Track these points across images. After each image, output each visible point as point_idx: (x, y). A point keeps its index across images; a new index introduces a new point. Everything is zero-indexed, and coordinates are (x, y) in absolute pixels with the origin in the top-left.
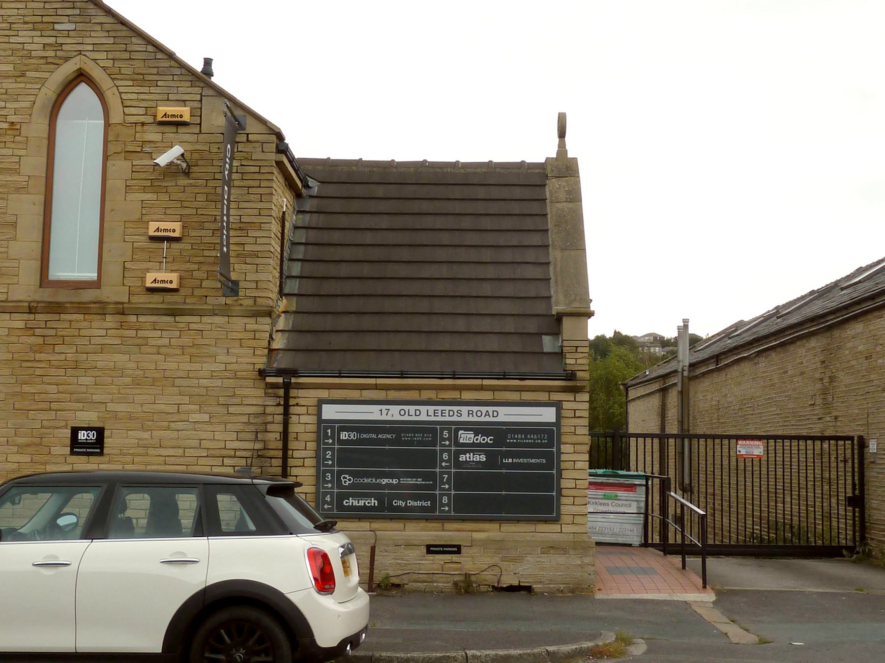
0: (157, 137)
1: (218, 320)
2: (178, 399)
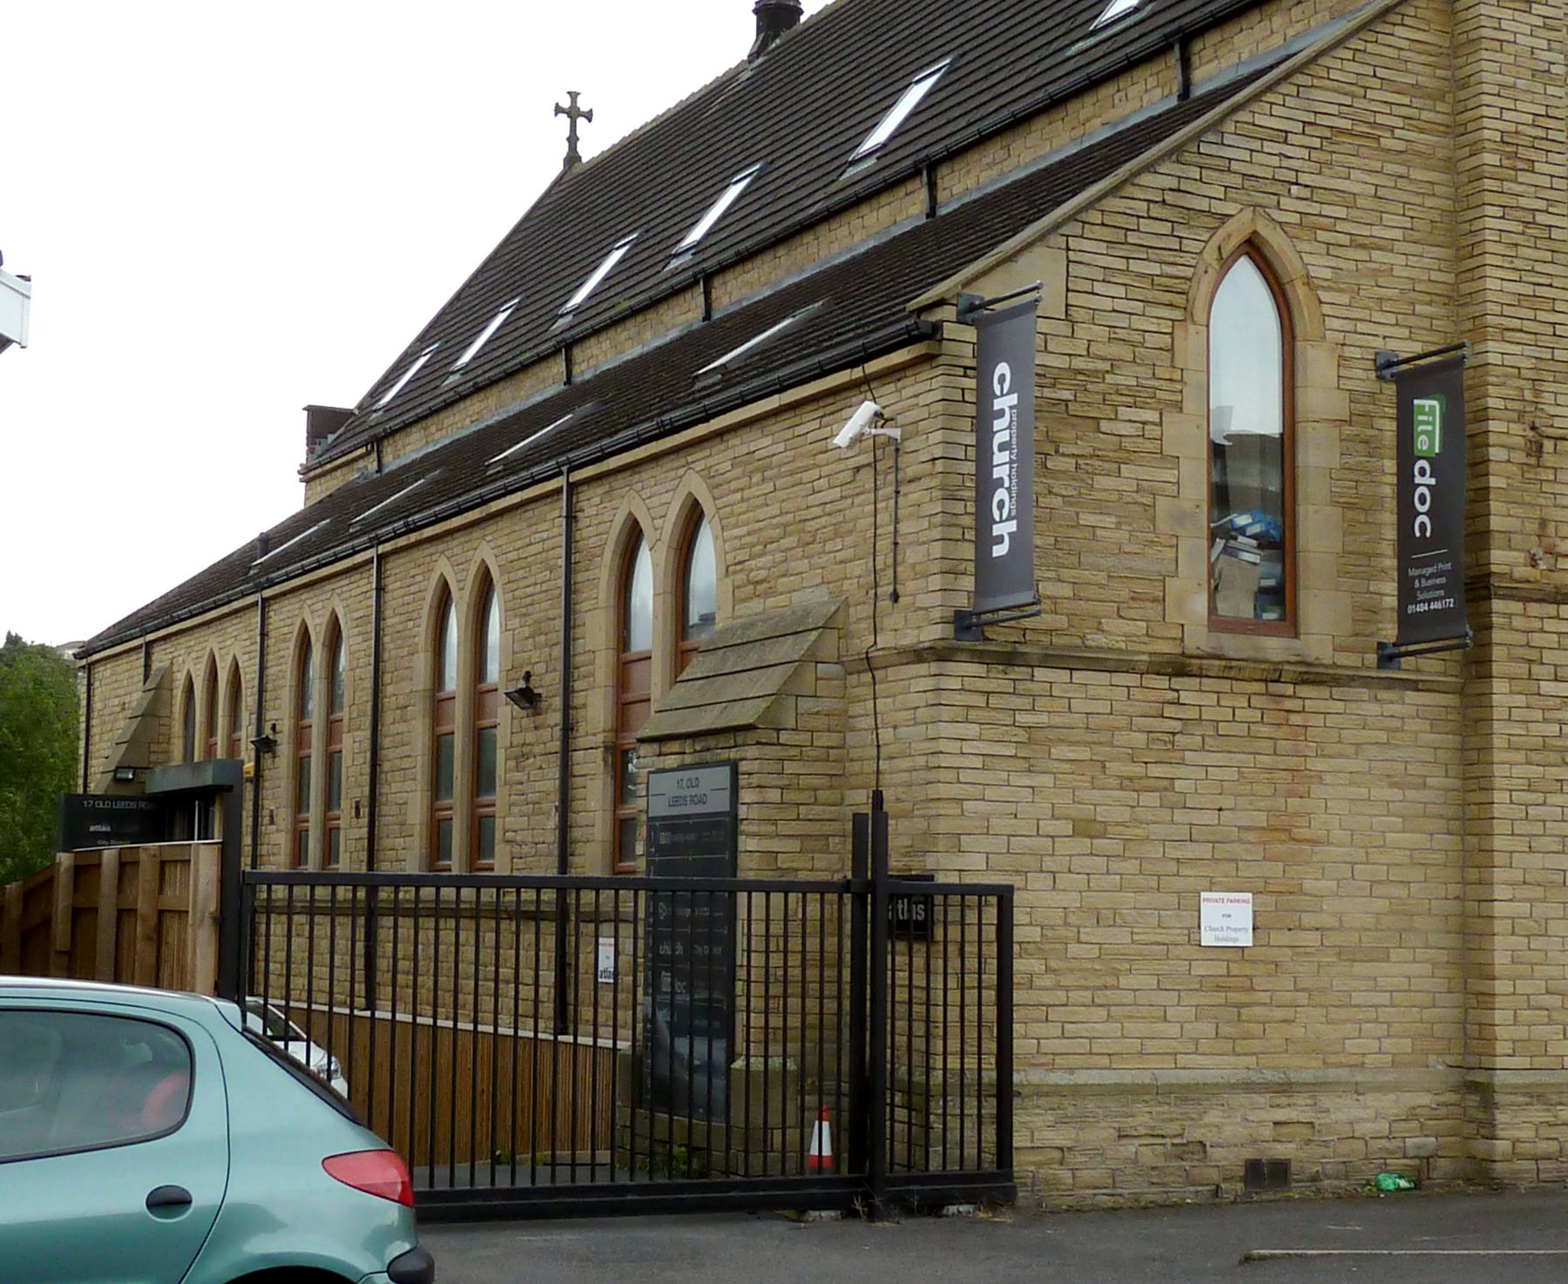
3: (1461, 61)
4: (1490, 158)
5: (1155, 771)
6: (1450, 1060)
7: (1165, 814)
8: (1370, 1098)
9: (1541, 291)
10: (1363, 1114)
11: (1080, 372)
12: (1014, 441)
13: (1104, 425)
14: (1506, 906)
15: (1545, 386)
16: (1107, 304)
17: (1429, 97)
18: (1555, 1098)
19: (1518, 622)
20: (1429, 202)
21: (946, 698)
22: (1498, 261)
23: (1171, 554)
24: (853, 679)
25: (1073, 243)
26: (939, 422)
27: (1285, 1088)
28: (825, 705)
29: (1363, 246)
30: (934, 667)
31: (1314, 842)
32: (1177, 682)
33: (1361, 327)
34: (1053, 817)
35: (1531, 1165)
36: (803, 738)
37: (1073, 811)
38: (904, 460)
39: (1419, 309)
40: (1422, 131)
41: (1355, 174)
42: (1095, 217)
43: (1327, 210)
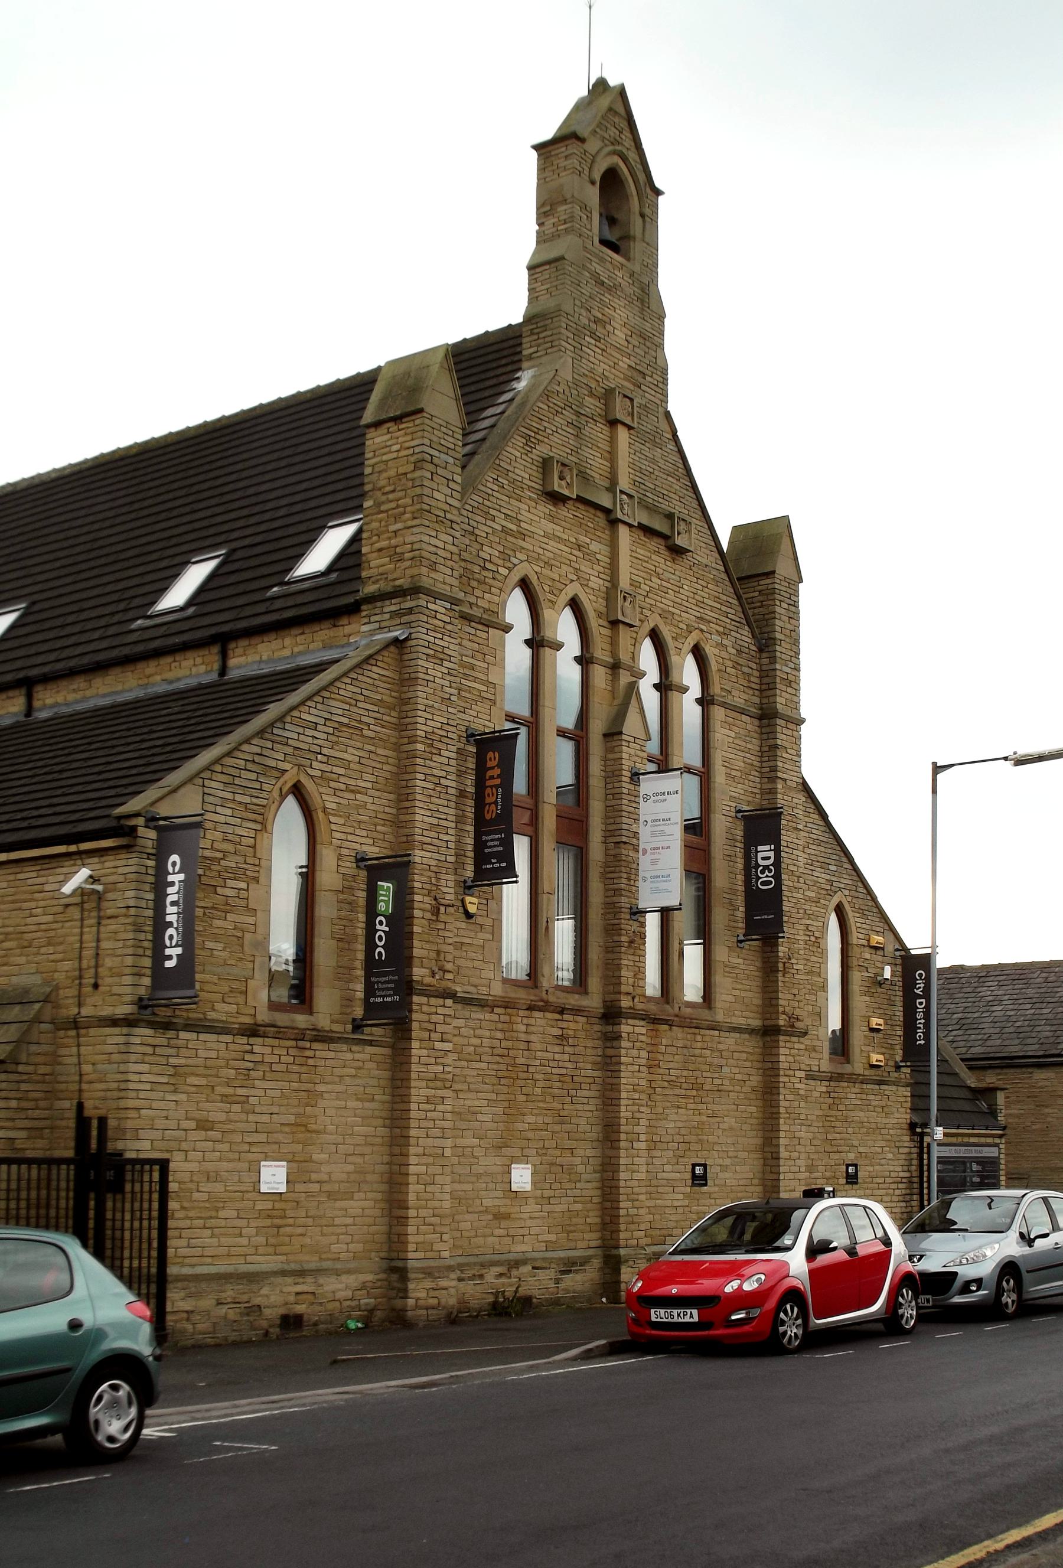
0: (868, 956)
1: (894, 1088)
2: (883, 1144)
3: (405, 689)
4: (420, 747)
5: (240, 1091)
6: (383, 1255)
7: (243, 1116)
8: (344, 1278)
9: (442, 823)
10: (340, 1286)
11: (206, 858)
12: (181, 901)
13: (219, 890)
14: (415, 1168)
15: (442, 876)
16: (222, 819)
17: (388, 708)
18: (437, 1275)
19: (425, 1009)
20: (386, 767)
21: (133, 1049)
22: (421, 805)
23: (250, 965)
24: (62, 1033)
25: (207, 783)
26: (134, 885)
27: (301, 1273)
28: (45, 1048)
29: (352, 791)
30: (125, 1030)
31: (318, 1132)
32: (252, 1040)
33: (350, 838)
34: (187, 1119)
35: (424, 1312)
36: (31, 1068)
37: (198, 1115)
38: (104, 904)
39: (379, 828)
40: (383, 727)
41: (350, 750)
42: (218, 768)
43: (336, 770)
